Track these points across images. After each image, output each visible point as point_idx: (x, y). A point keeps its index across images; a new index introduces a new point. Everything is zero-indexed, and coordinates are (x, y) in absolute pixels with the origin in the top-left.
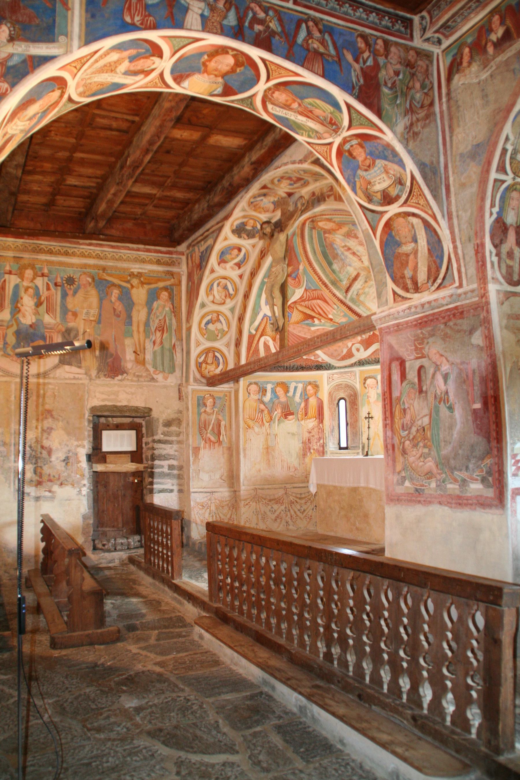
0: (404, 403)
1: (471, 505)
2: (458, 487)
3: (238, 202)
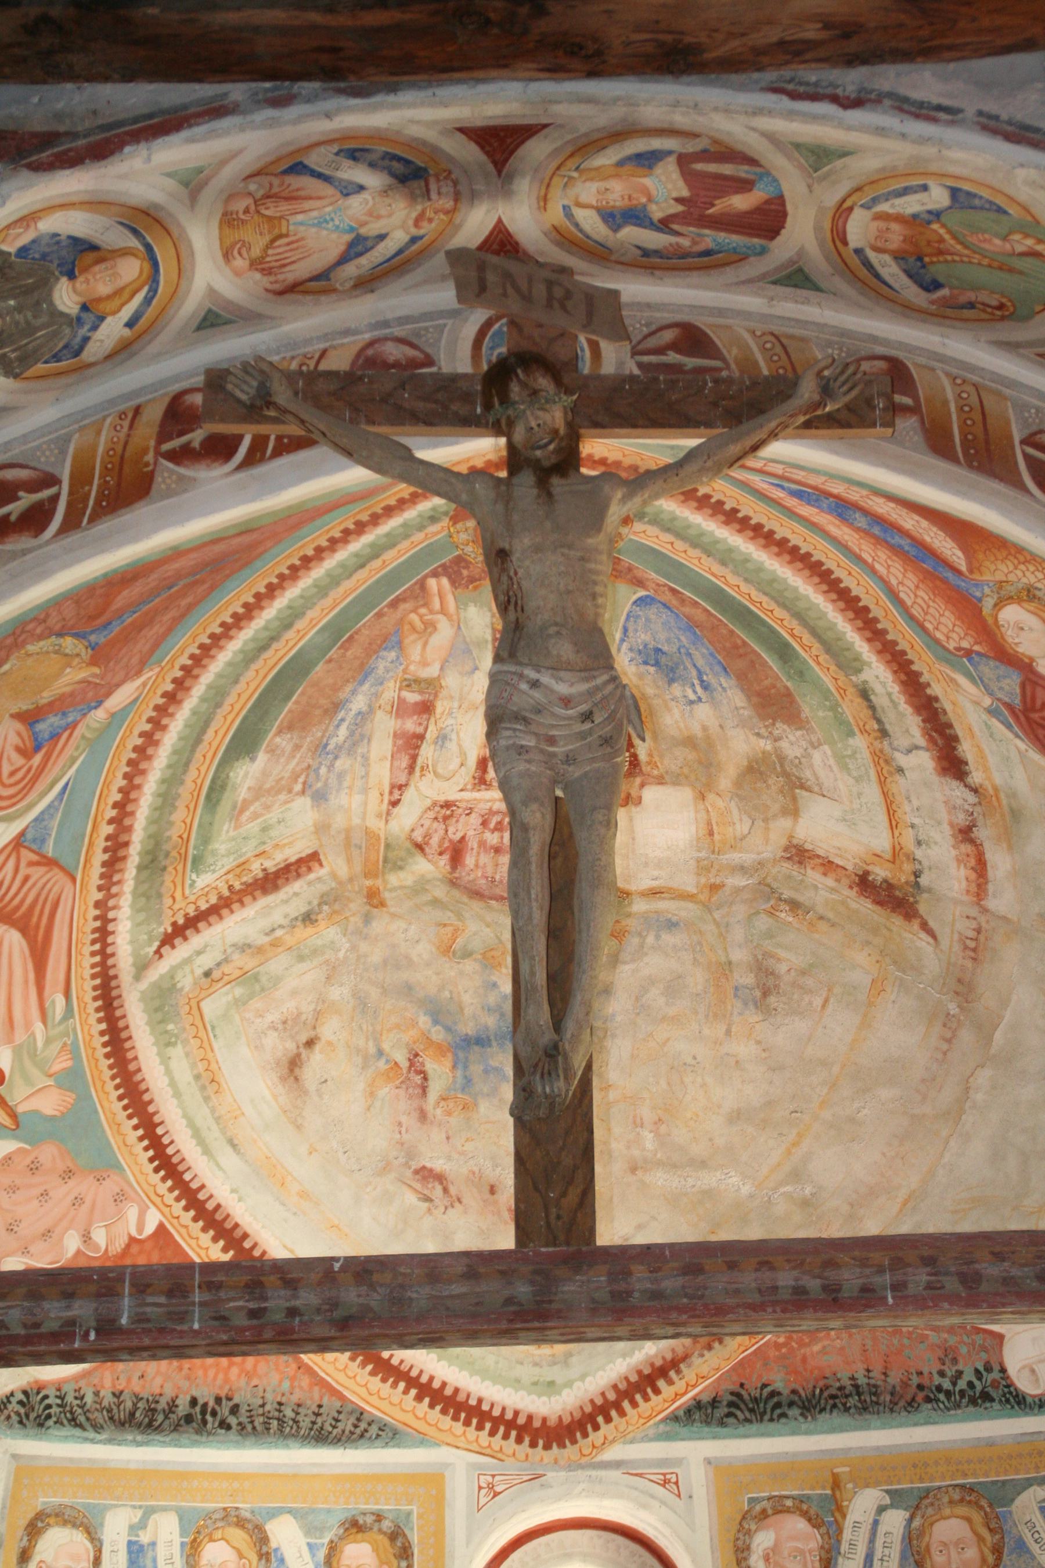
3: (217, 111)
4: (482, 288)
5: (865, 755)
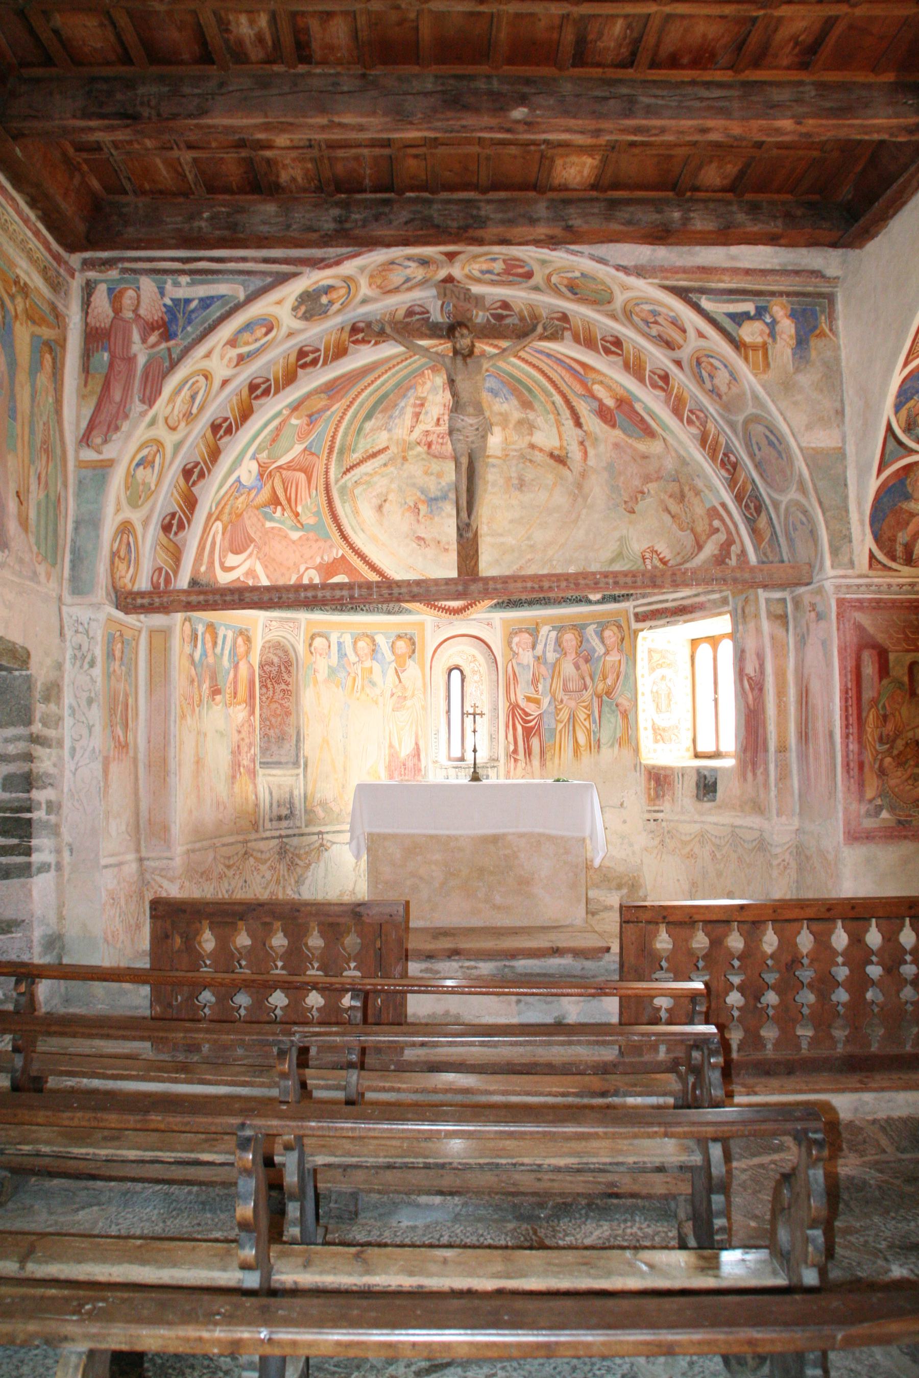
4: (445, 295)
5: (553, 420)
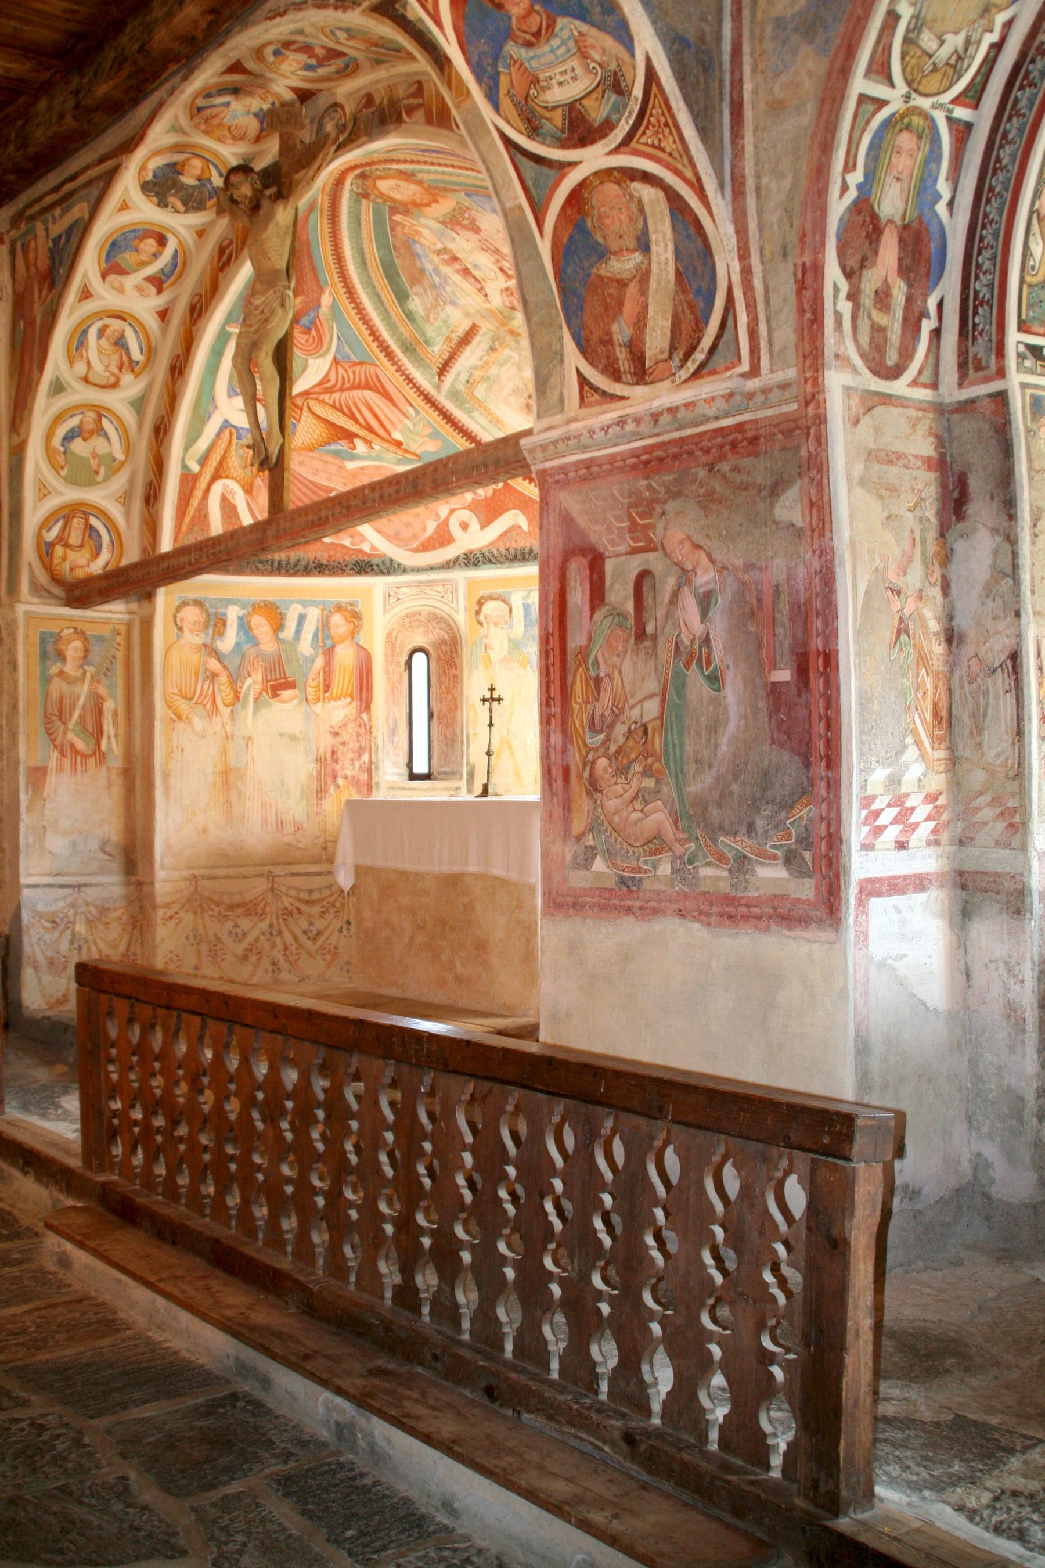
0: (596, 662)
1: (759, 918)
2: (726, 874)
3: (160, 105)
